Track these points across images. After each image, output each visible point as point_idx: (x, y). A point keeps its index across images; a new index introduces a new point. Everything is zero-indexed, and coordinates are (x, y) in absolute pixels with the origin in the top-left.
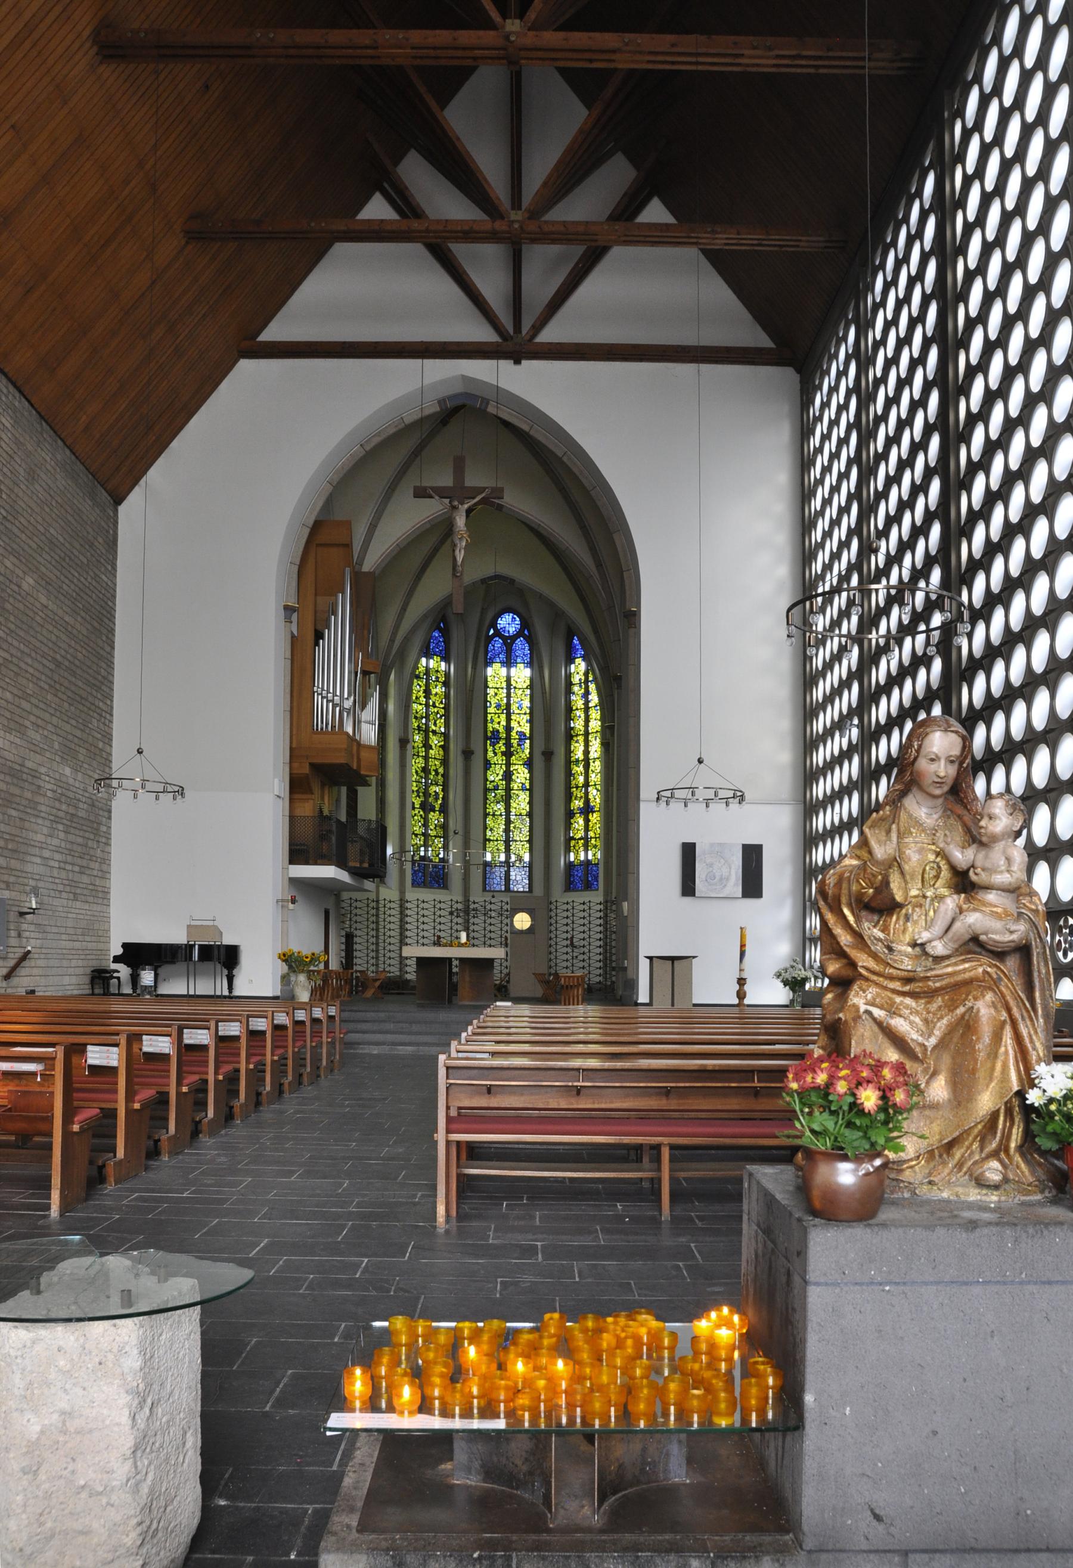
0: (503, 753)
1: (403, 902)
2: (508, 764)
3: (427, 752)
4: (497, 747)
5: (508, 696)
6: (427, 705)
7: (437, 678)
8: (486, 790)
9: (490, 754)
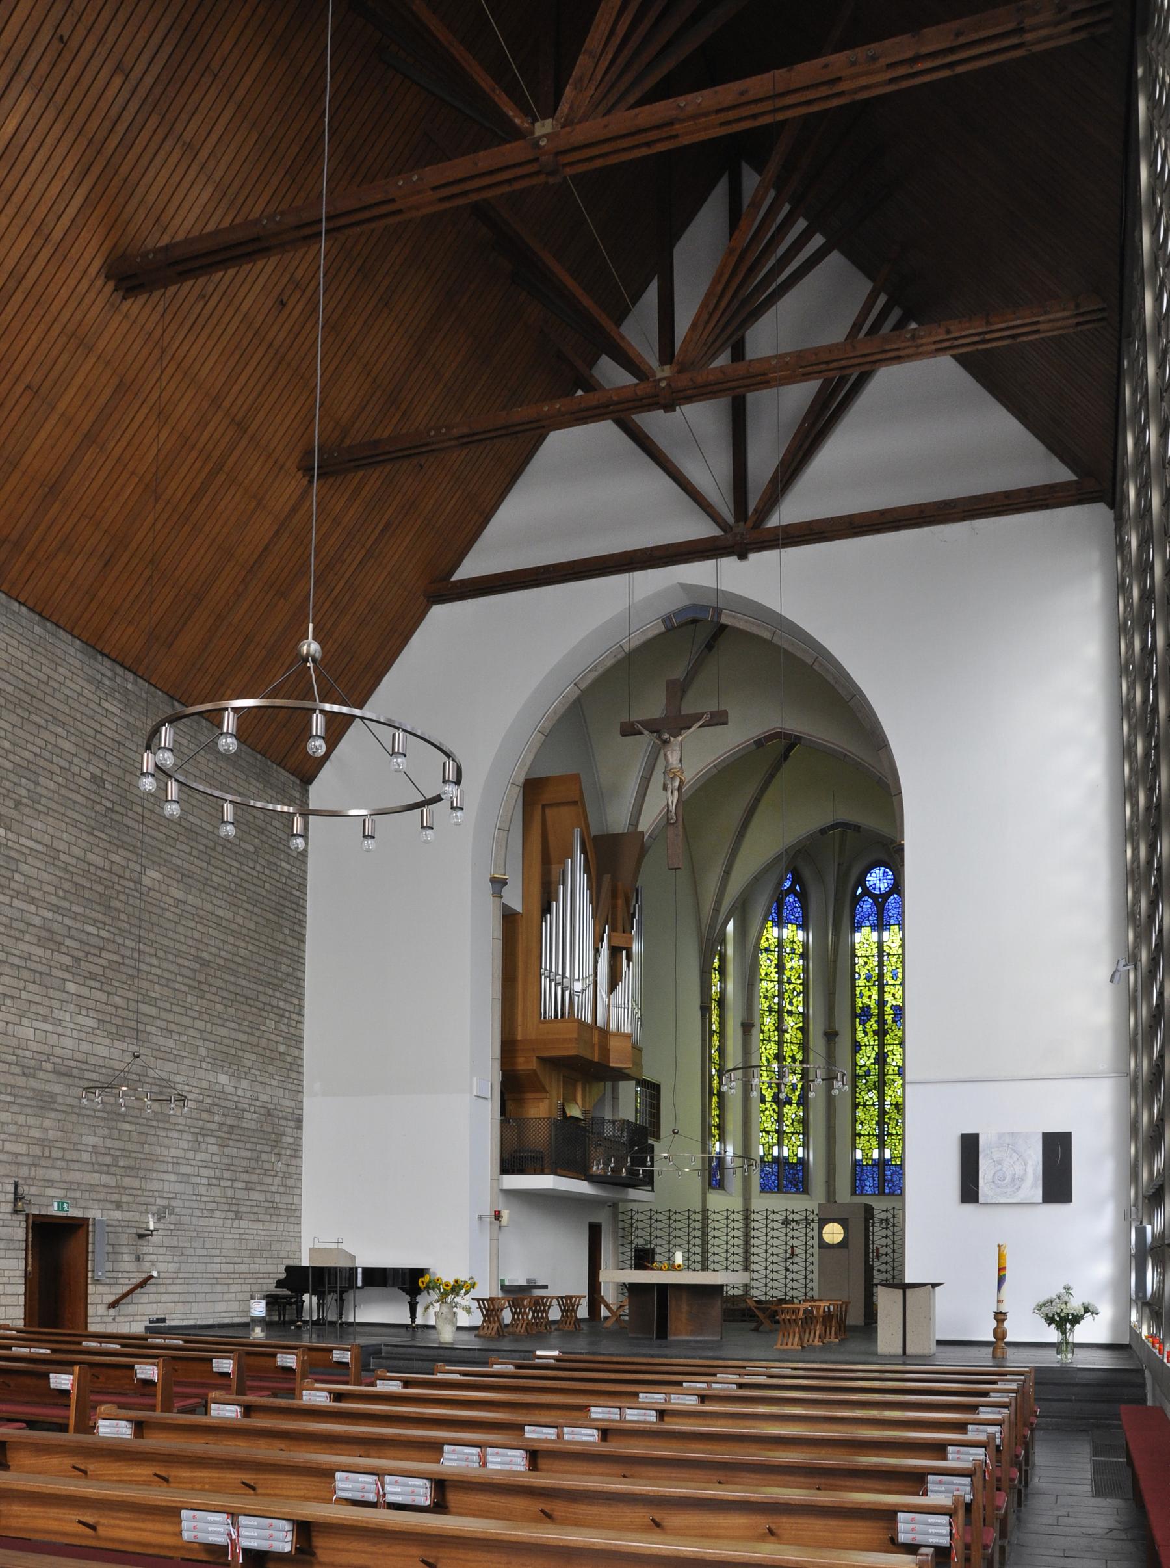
0: (875, 1033)
1: (747, 1213)
2: (882, 1045)
3: (781, 1036)
4: (868, 1025)
5: (881, 965)
6: (780, 982)
7: (793, 949)
8: (855, 1077)
9: (860, 1034)
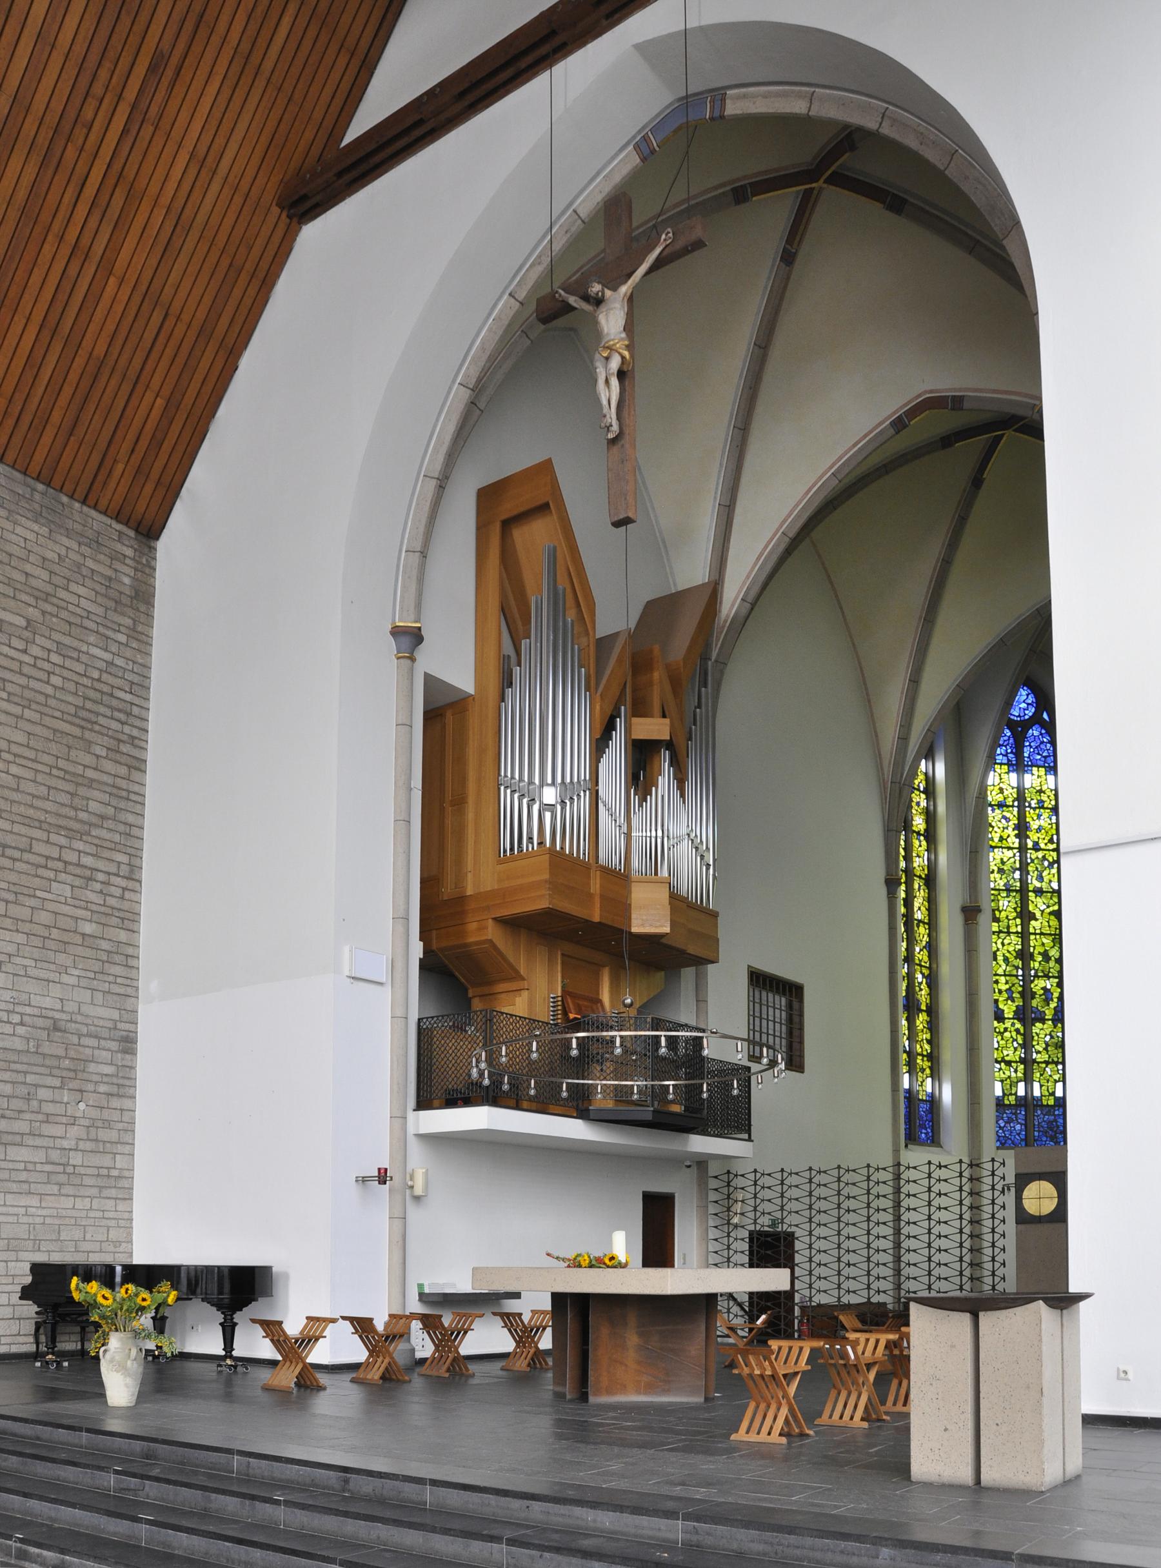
3: (1025, 926)
6: (1022, 849)
7: (1041, 802)
